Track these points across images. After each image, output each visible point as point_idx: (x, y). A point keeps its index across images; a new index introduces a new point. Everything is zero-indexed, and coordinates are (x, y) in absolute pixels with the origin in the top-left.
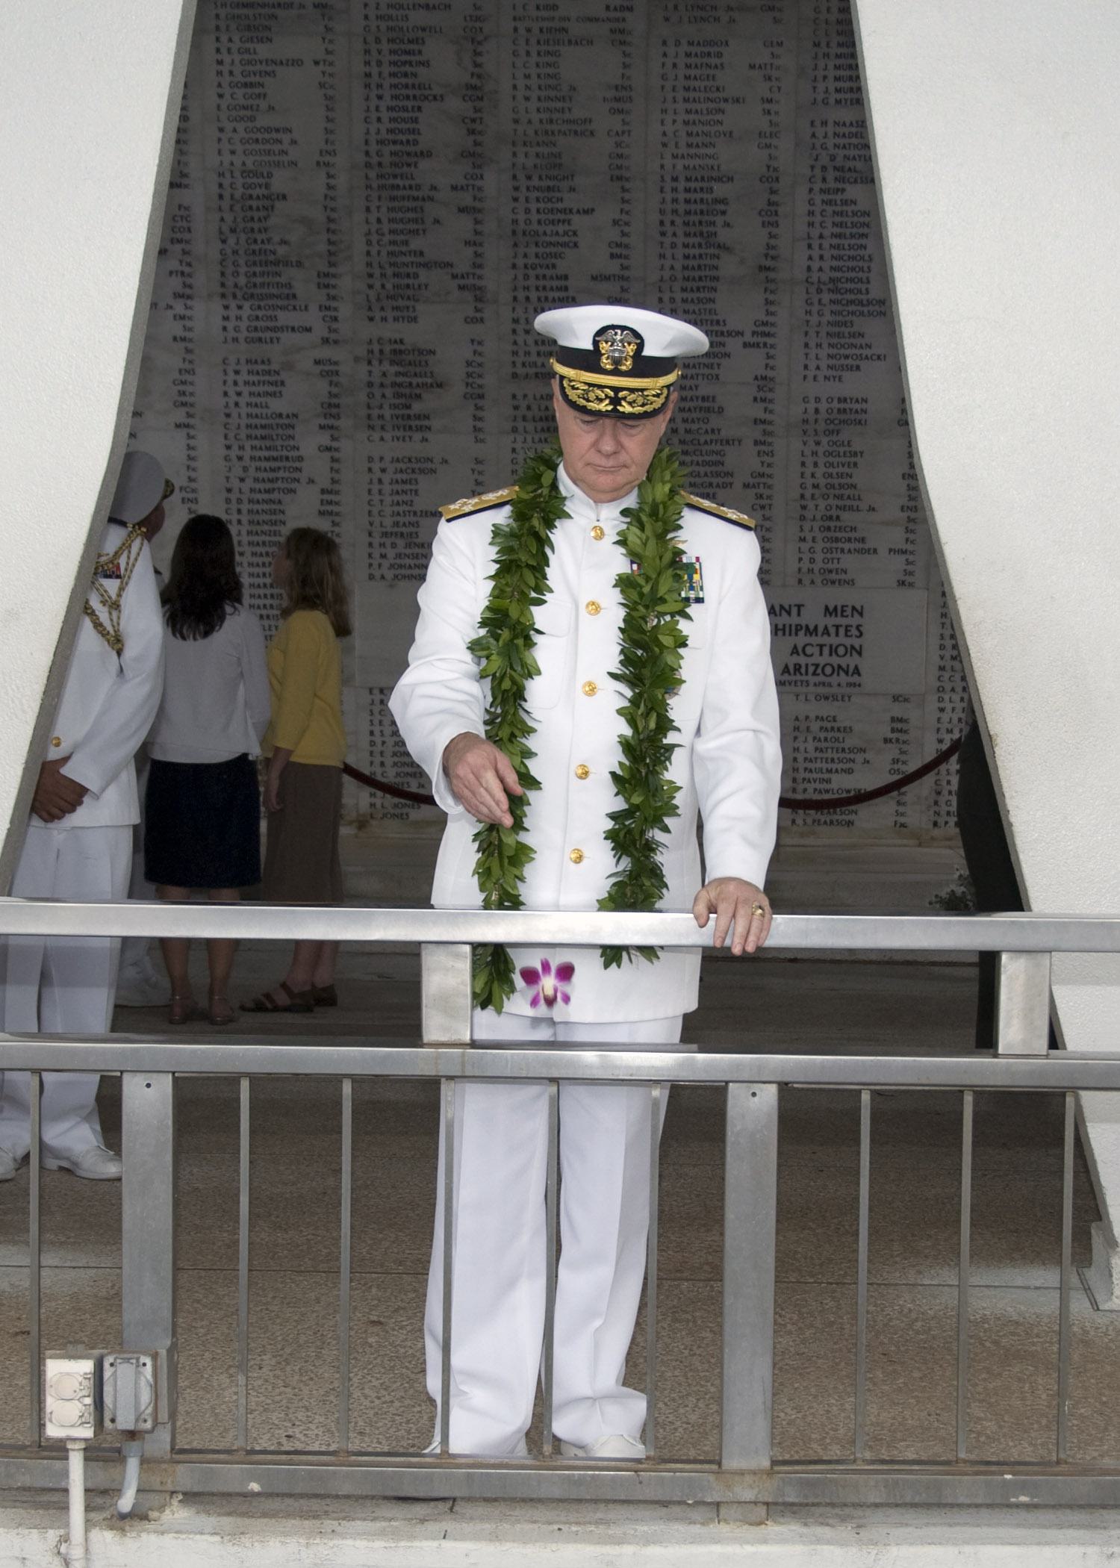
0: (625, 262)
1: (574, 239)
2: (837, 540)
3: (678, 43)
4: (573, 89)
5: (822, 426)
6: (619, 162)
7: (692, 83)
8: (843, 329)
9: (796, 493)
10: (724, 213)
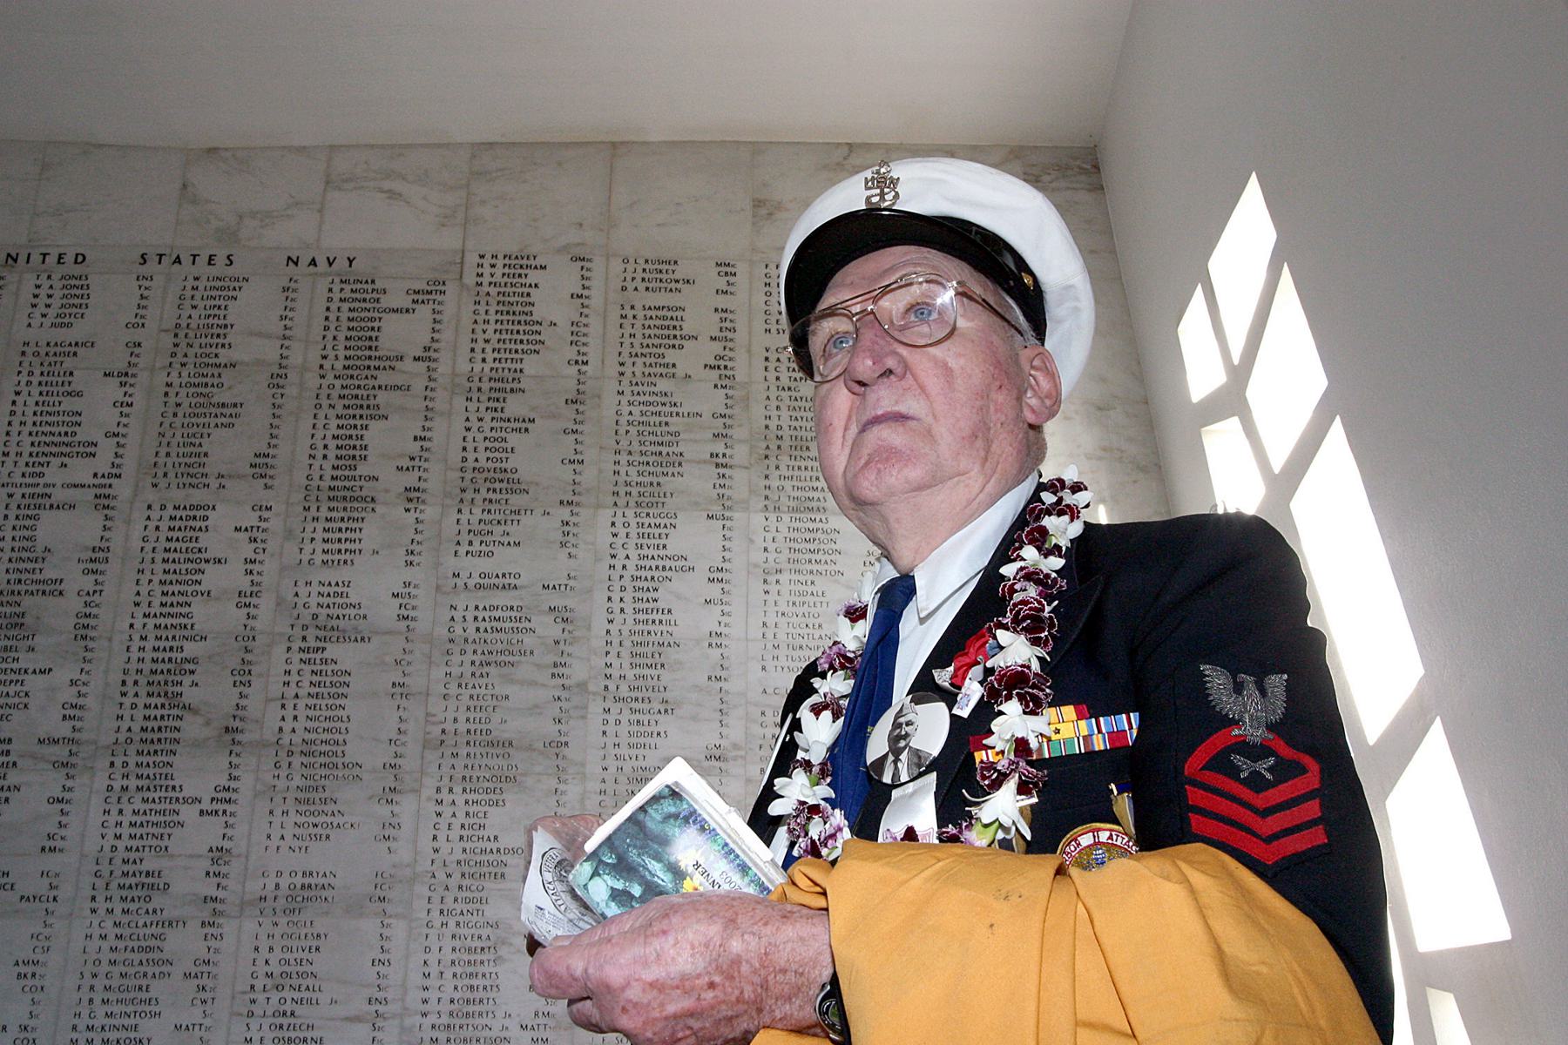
0: (78, 724)
1: (25, 700)
3: (163, 508)
4: (47, 550)
6: (86, 621)
7: (173, 545)
9: (243, 986)
10: (192, 672)
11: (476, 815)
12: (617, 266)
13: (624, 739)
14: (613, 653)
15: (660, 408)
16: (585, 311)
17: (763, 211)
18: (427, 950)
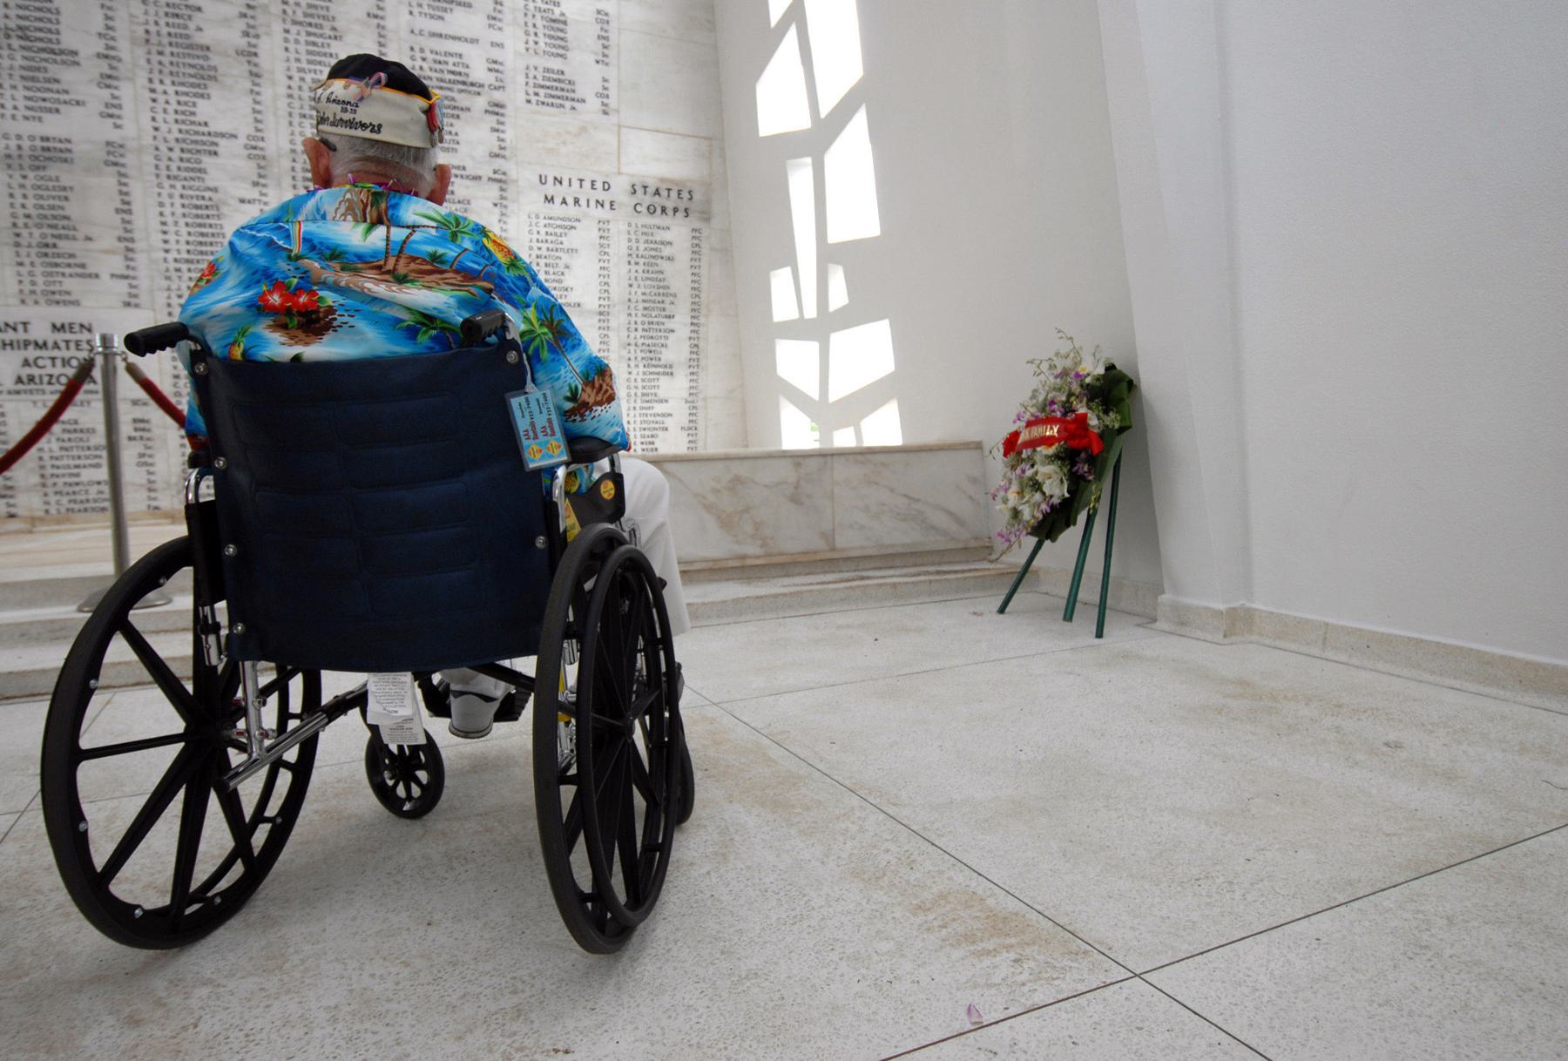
2: (57, 265)
5: (27, 162)
8: (37, 74)
11: (186, 104)
13: (304, 57)
18: (161, 204)
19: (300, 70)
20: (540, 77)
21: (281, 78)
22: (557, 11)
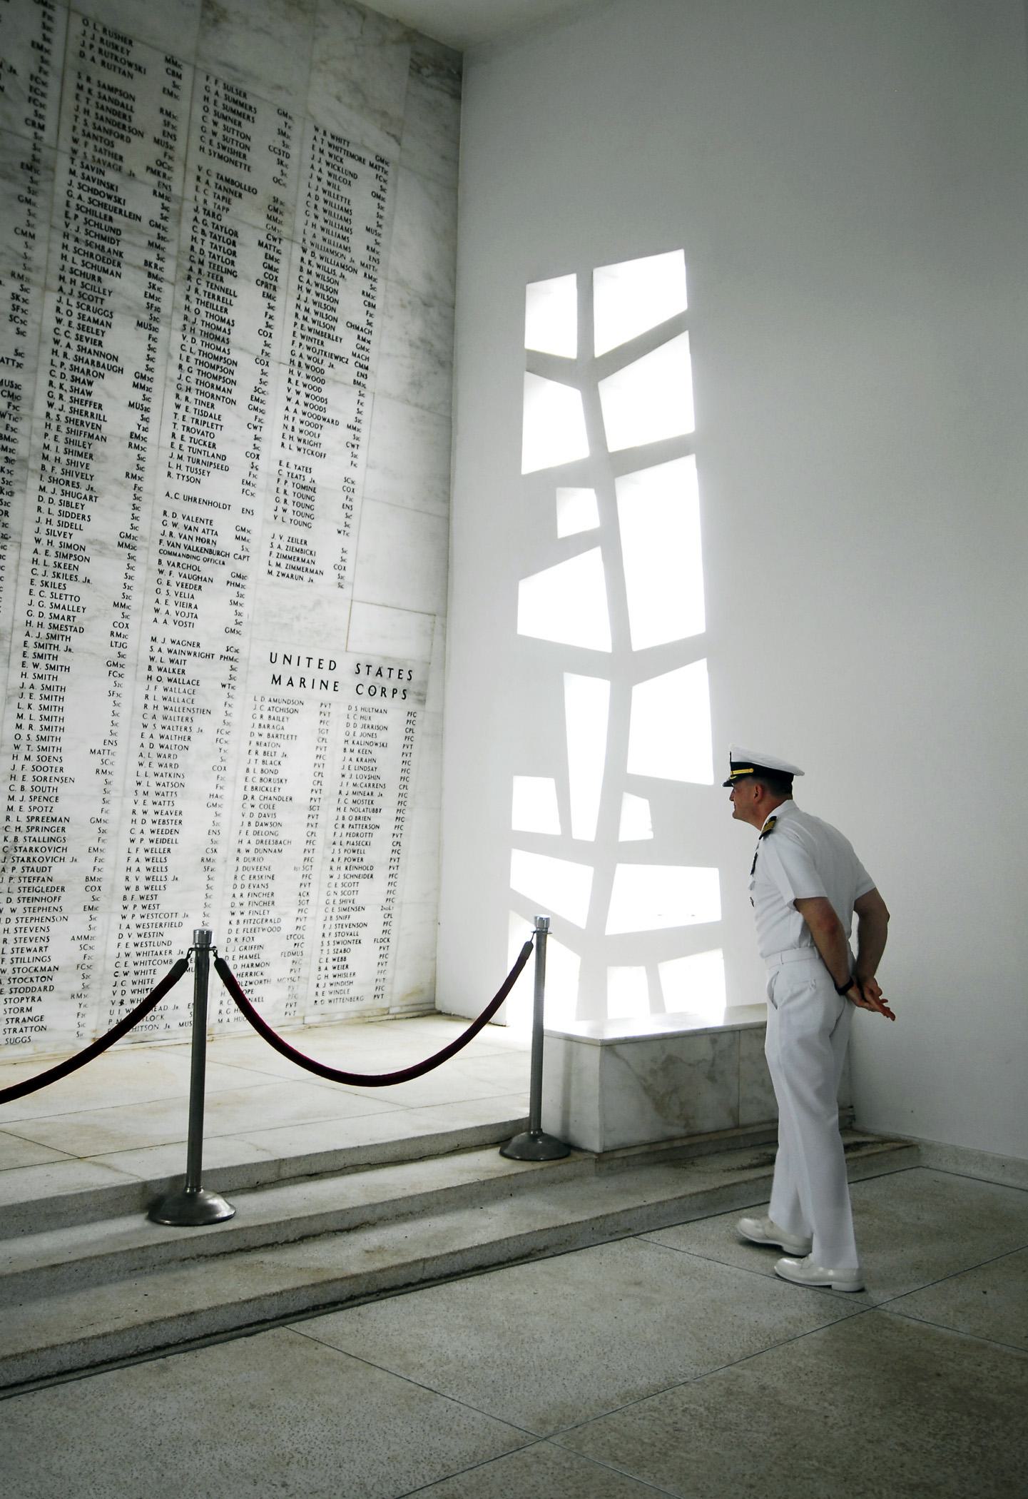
12: (77, 27)
13: (55, 522)
14: (51, 435)
15: (105, 200)
16: (45, 67)
17: (210, 15)
19: (49, 533)
20: (283, 547)
21: (29, 540)
22: (308, 477)
